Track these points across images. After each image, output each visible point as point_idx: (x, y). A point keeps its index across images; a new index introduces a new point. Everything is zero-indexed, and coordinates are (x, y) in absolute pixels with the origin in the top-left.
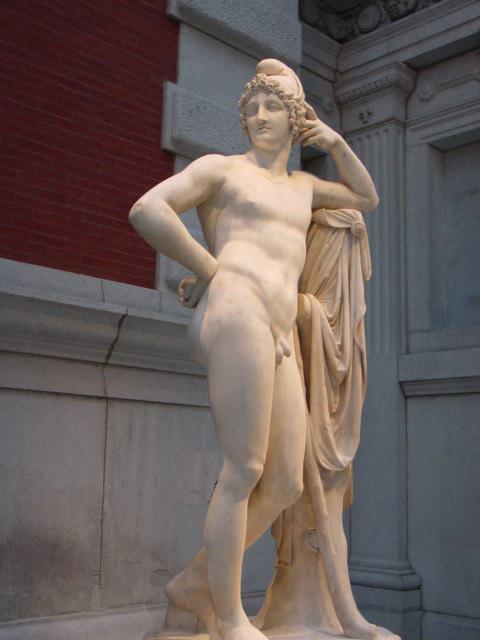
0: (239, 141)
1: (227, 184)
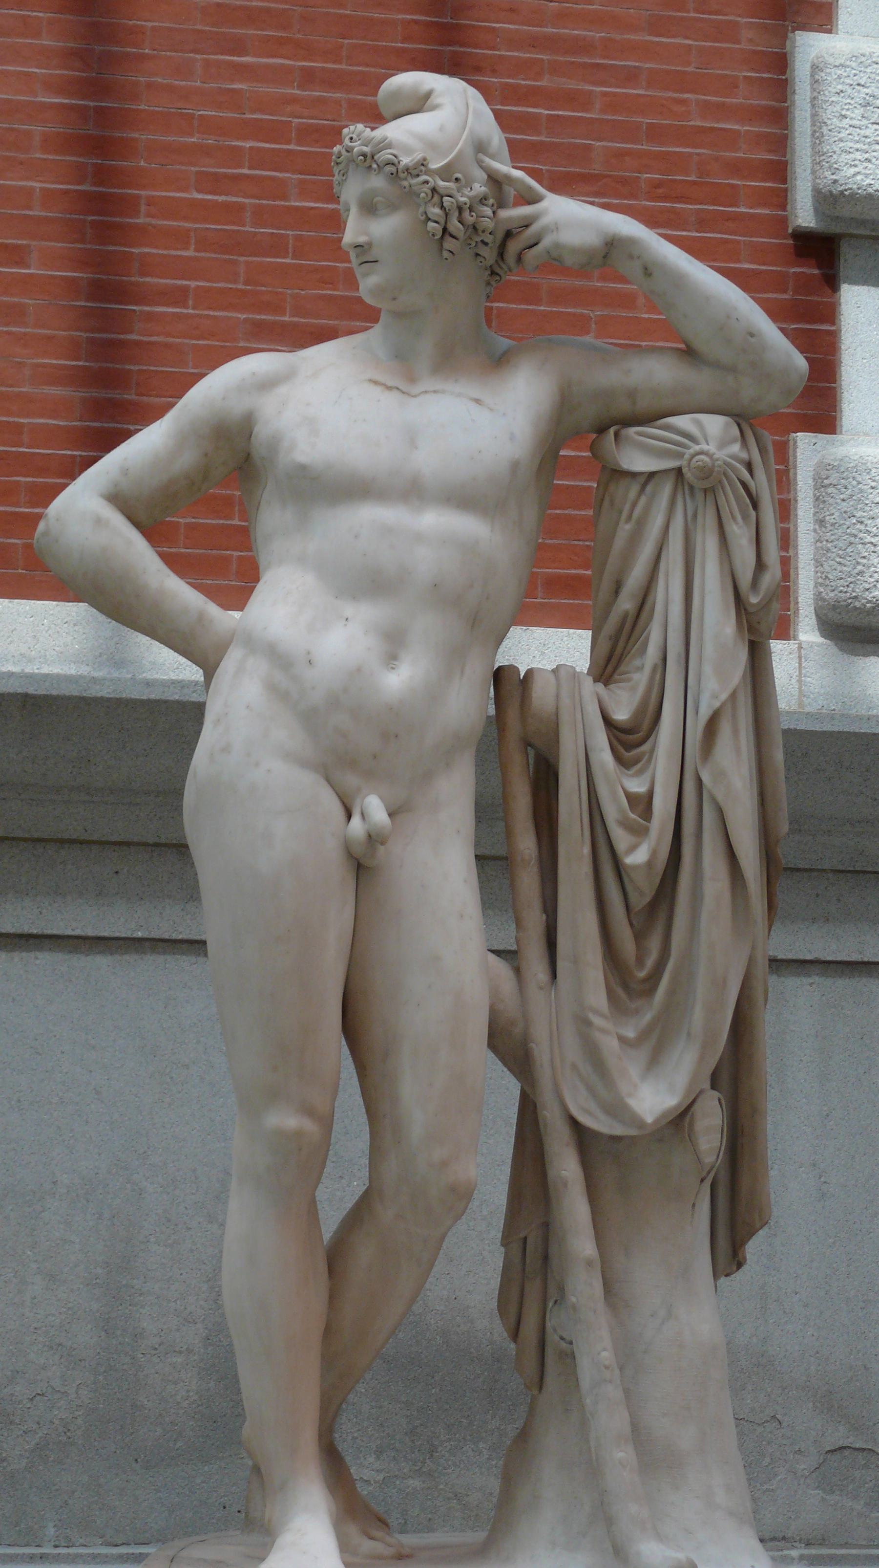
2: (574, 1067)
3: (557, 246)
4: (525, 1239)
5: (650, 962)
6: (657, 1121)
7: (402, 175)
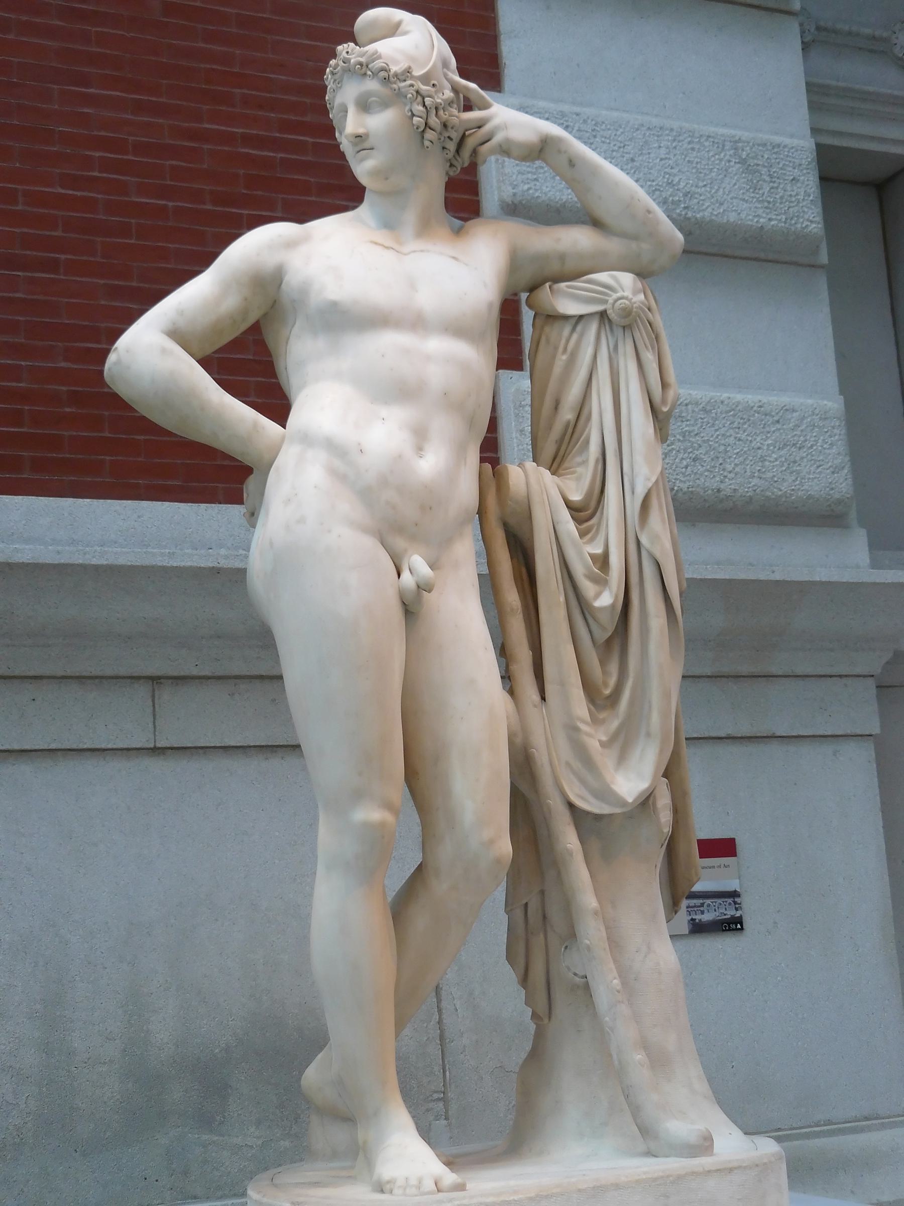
1: (287, 279)
2: (568, 764)
3: (508, 141)
4: (526, 905)
5: (612, 681)
6: (635, 801)
7: (392, 79)
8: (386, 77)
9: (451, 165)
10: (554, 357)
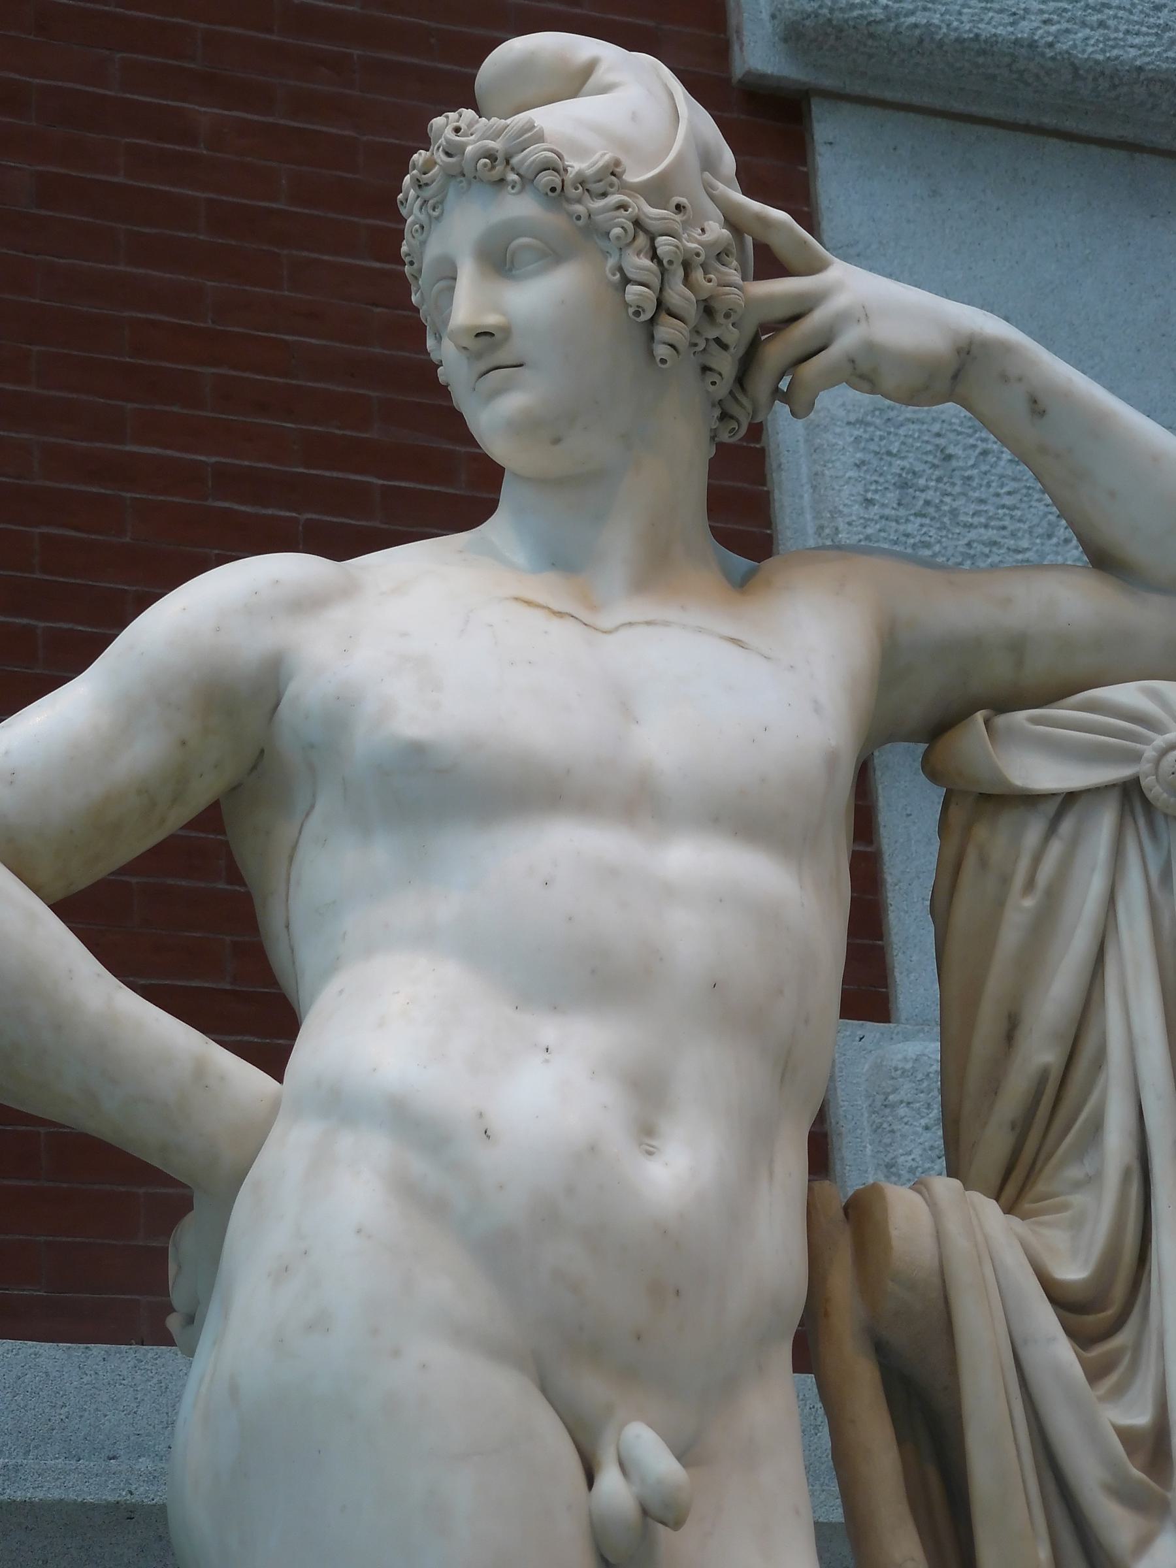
0: (402, 473)
3: (871, 348)
7: (571, 192)
8: (556, 185)
9: (725, 416)
10: (1000, 904)
